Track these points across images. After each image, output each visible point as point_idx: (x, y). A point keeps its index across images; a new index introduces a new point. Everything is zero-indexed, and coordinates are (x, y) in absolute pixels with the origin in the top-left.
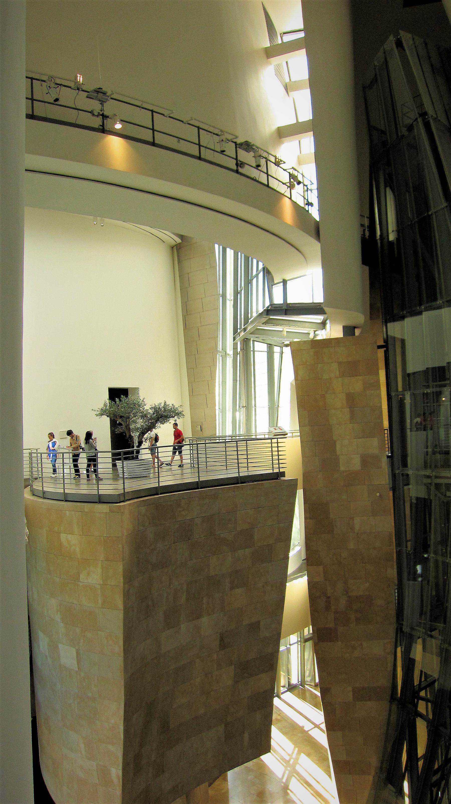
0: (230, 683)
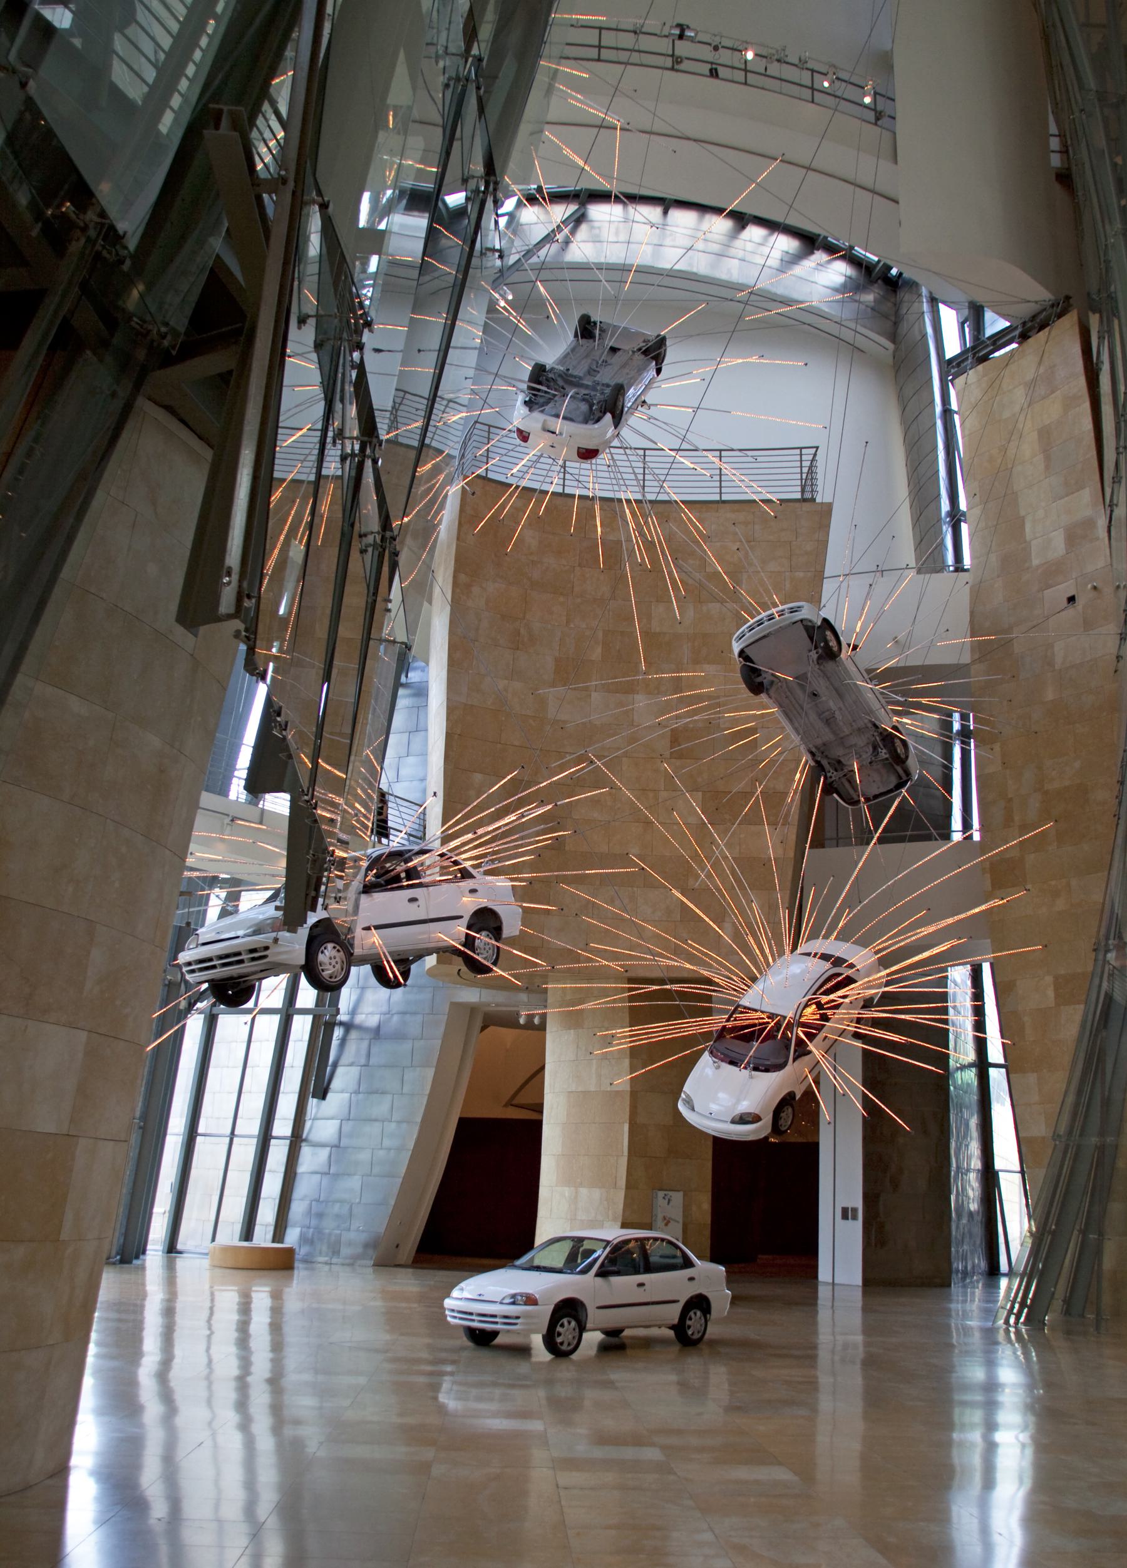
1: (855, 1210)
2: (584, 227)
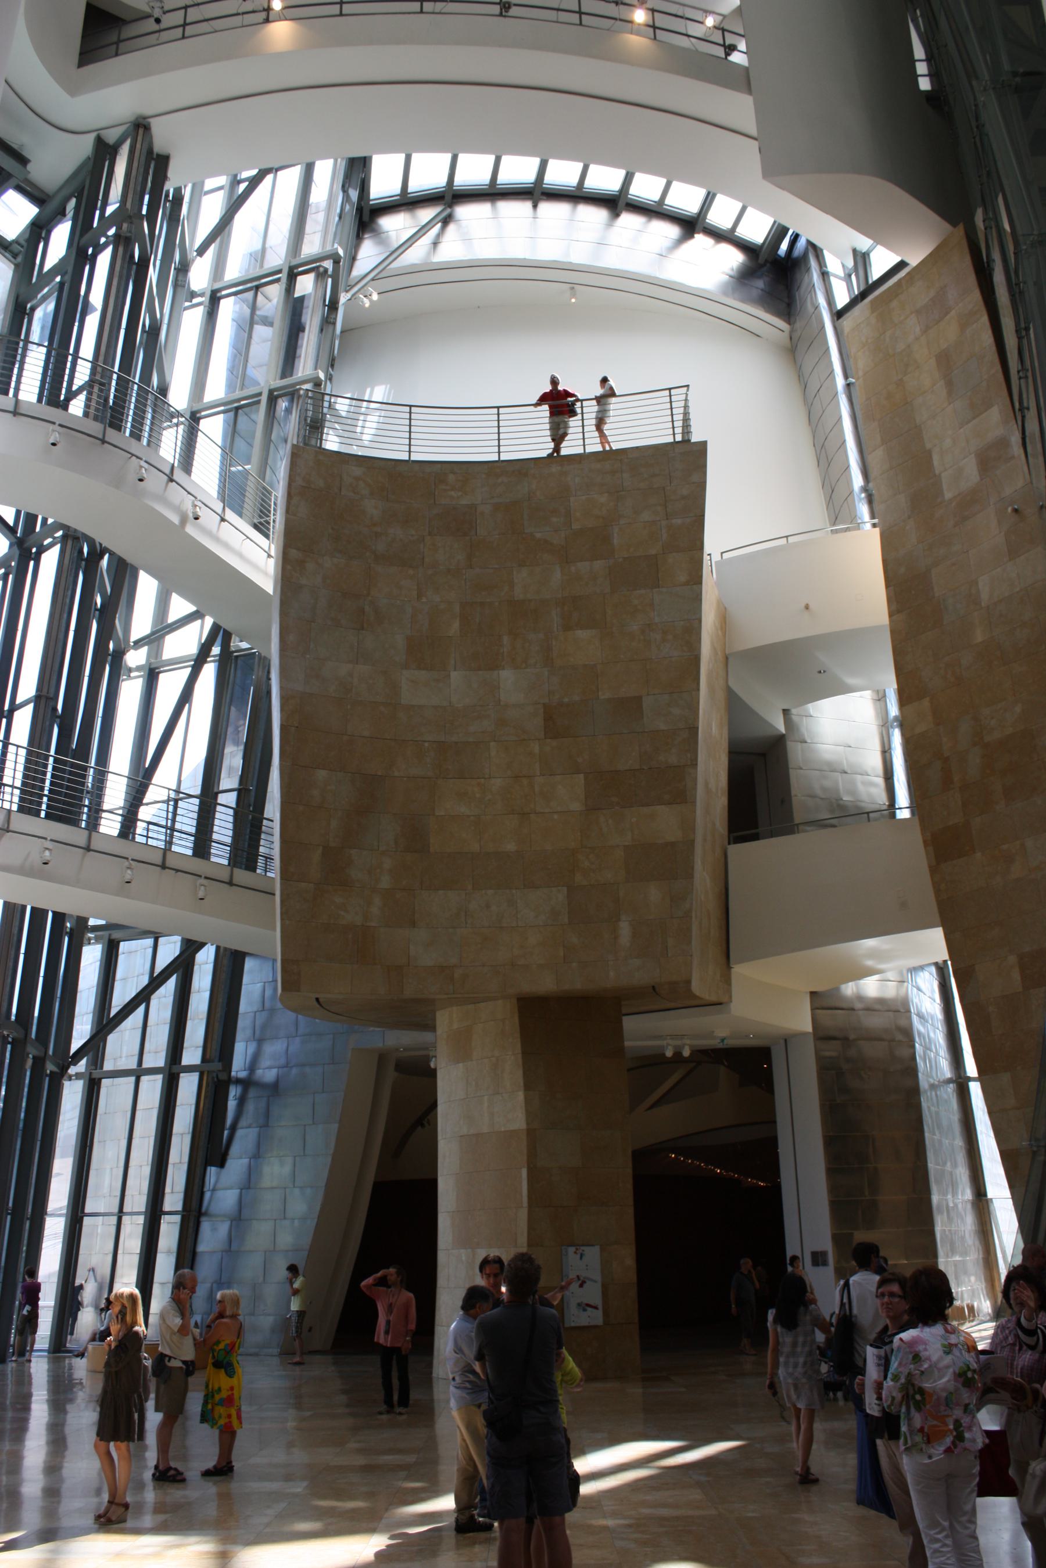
0: (576, 806)
1: (824, 1254)
2: (451, 228)
